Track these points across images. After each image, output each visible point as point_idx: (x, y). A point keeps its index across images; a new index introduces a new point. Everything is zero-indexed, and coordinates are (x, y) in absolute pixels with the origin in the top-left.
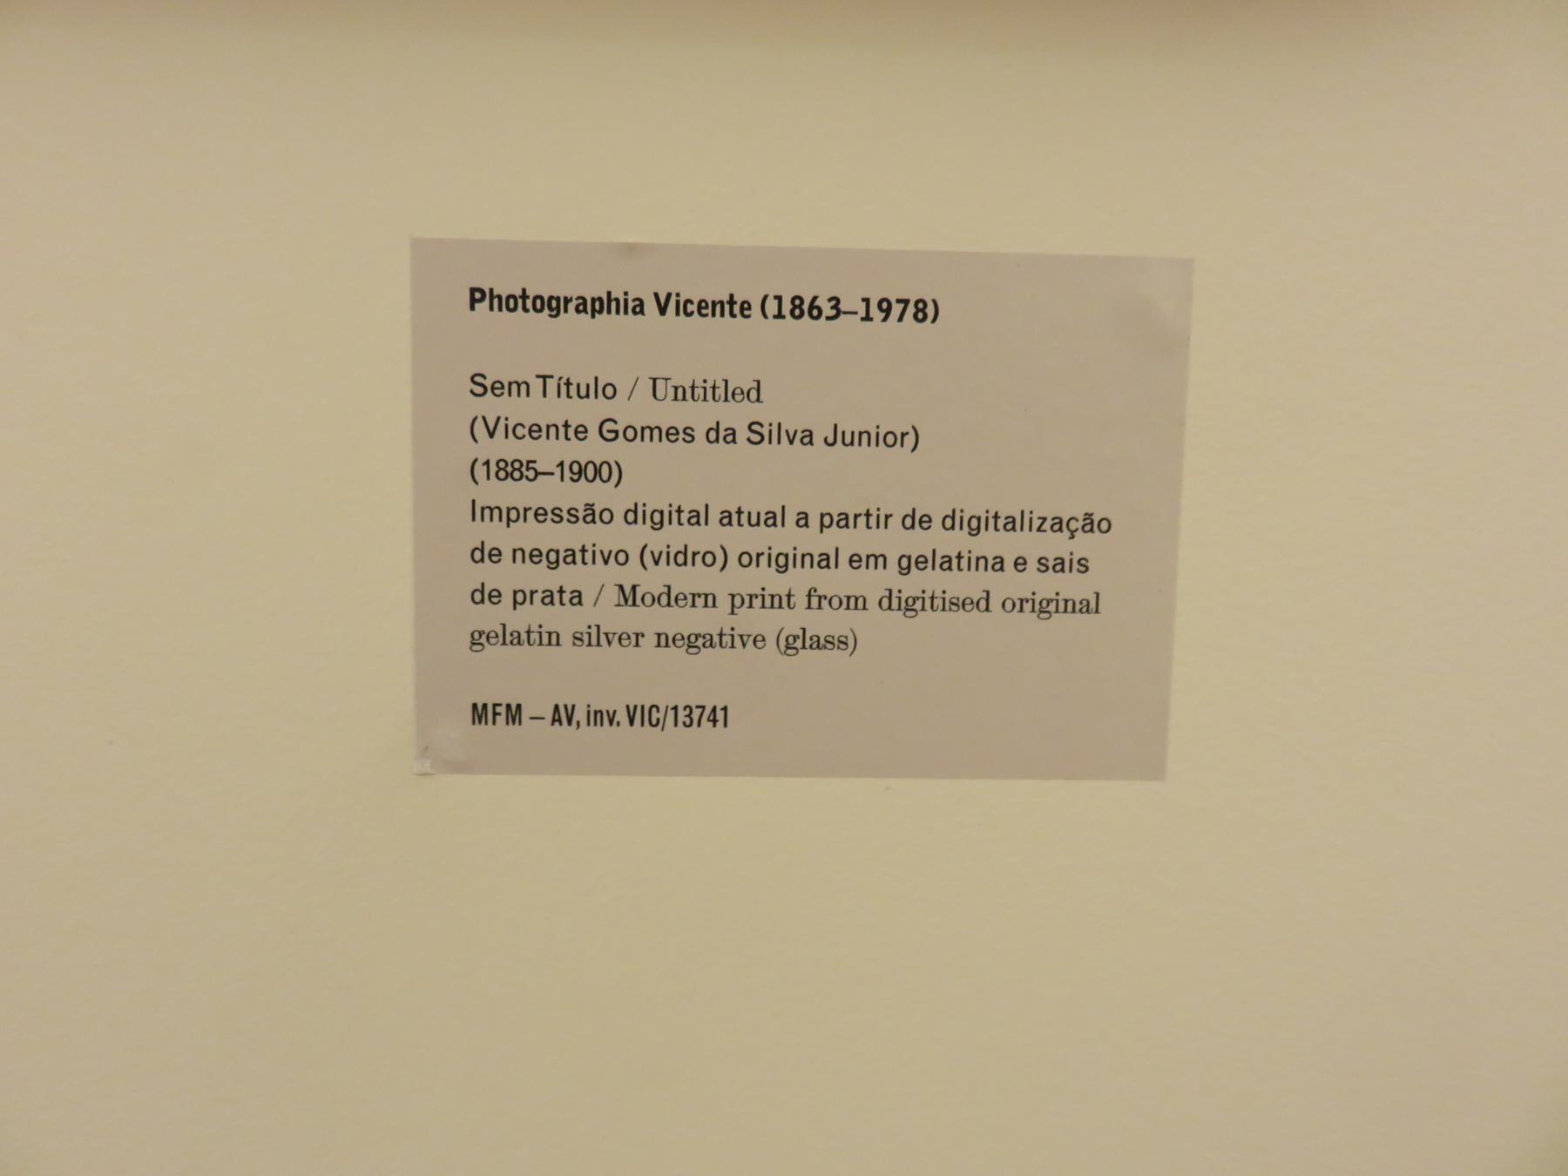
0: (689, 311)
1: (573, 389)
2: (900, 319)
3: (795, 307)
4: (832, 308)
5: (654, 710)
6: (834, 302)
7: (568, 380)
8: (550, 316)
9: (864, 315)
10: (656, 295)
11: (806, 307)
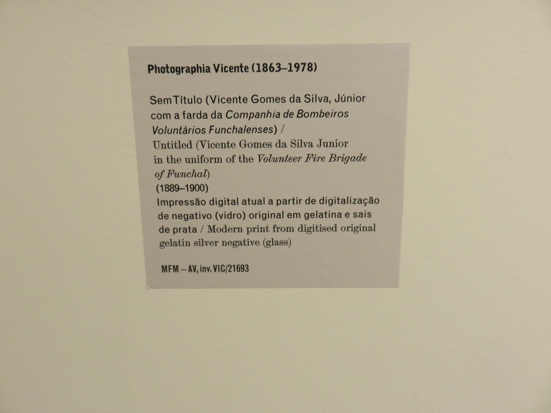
0: (226, 70)
1: (187, 101)
2: (303, 70)
3: (264, 67)
4: (278, 67)
5: (223, 266)
6: (278, 65)
7: (185, 97)
8: (177, 74)
10: (214, 65)
11: (268, 67)
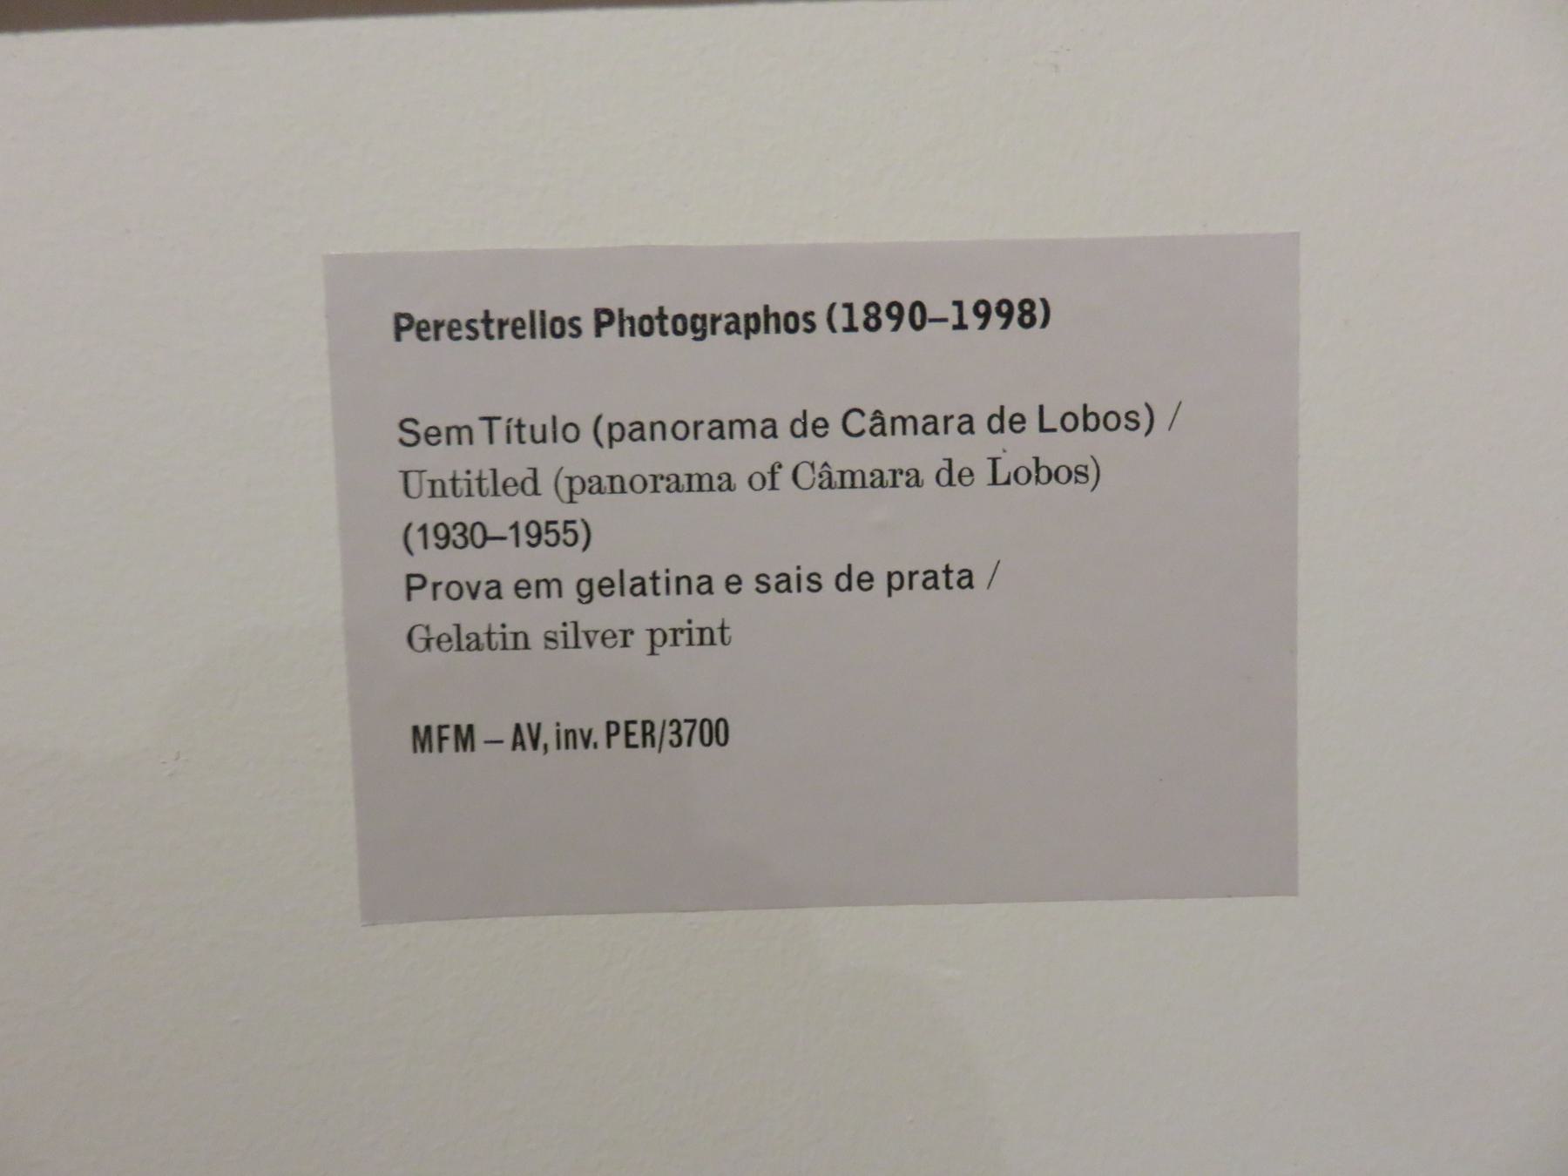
9: (956, 323)
